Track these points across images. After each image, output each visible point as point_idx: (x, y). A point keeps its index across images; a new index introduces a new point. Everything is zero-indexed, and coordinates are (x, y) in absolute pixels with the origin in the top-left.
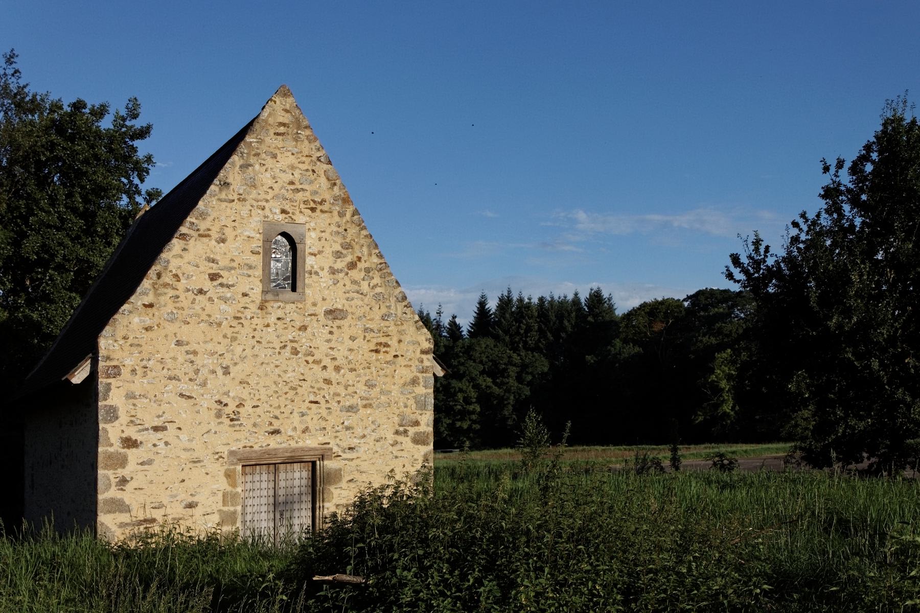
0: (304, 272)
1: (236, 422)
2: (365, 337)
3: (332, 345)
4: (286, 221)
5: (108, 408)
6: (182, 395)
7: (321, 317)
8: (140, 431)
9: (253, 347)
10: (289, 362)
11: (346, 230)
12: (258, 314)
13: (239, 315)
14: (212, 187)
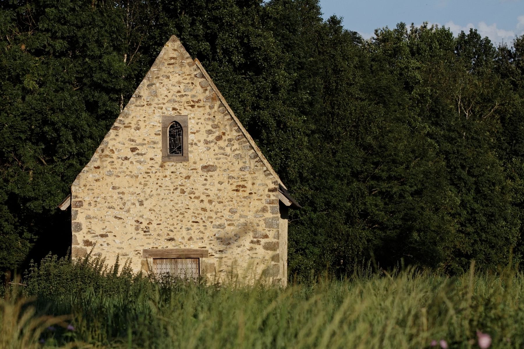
0: (188, 144)
1: (147, 233)
2: (229, 182)
3: (207, 187)
4: (176, 114)
5: (76, 224)
6: (116, 217)
7: (199, 170)
8: (93, 237)
9: (157, 189)
10: (179, 198)
11: (214, 117)
12: (159, 170)
13: (149, 171)
14: (132, 99)
